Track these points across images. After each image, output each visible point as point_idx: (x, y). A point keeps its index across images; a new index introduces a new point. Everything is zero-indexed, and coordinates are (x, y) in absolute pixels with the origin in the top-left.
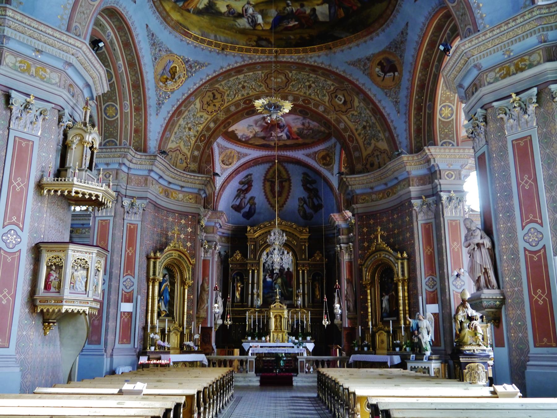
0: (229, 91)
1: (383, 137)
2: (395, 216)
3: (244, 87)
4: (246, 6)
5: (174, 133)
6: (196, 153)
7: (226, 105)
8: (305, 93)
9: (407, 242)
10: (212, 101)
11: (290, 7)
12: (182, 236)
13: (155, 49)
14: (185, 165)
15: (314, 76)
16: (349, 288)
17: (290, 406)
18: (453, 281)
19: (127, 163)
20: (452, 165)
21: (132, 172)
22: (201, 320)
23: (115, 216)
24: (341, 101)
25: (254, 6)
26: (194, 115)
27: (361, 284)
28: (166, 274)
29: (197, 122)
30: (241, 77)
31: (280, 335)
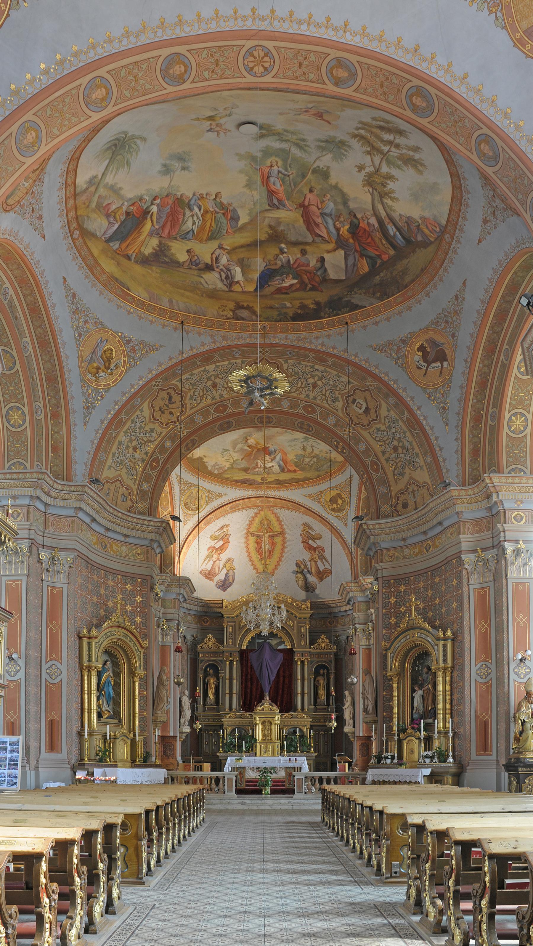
0: (192, 391)
1: (422, 463)
2: (437, 580)
3: (215, 385)
4: (218, 252)
5: (111, 455)
6: (145, 486)
7: (188, 412)
8: (307, 396)
9: (453, 615)
10: (167, 406)
11: (285, 255)
12: (129, 608)
13: (78, 320)
14: (129, 503)
15: (322, 368)
16: (368, 681)
17: (283, 833)
18: (515, 668)
19: (43, 497)
20: (522, 502)
21: (51, 510)
22: (160, 725)
23: (28, 575)
24: (360, 408)
26: (140, 428)
27: (385, 676)
28: (106, 661)
29: (145, 439)
30: (210, 368)
31: (270, 746)
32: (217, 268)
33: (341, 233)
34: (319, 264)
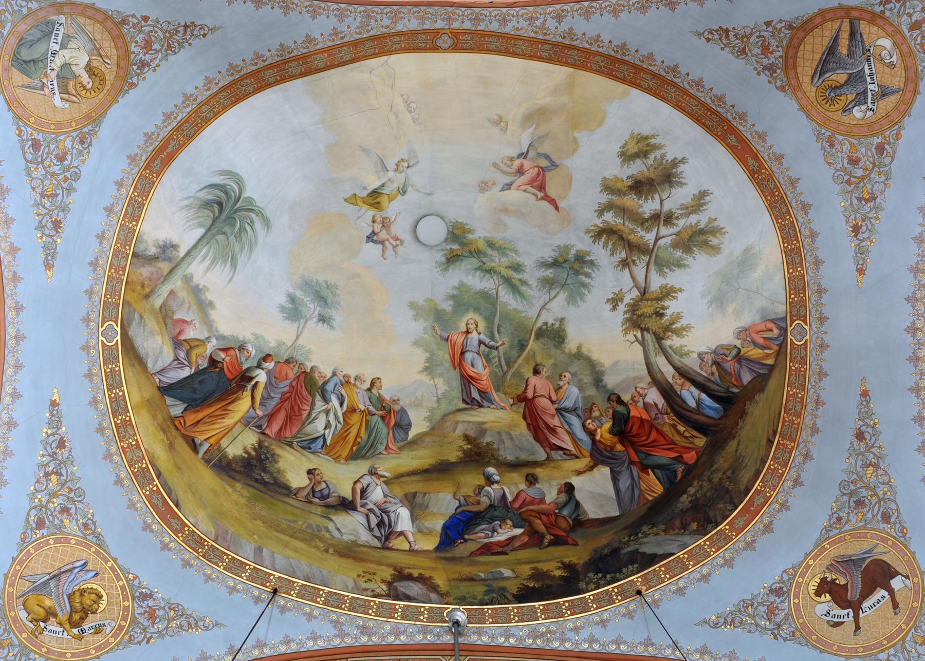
4: (366, 480)
11: (495, 486)
25: (388, 482)
32: (363, 506)
33: (598, 437)
34: (563, 498)
